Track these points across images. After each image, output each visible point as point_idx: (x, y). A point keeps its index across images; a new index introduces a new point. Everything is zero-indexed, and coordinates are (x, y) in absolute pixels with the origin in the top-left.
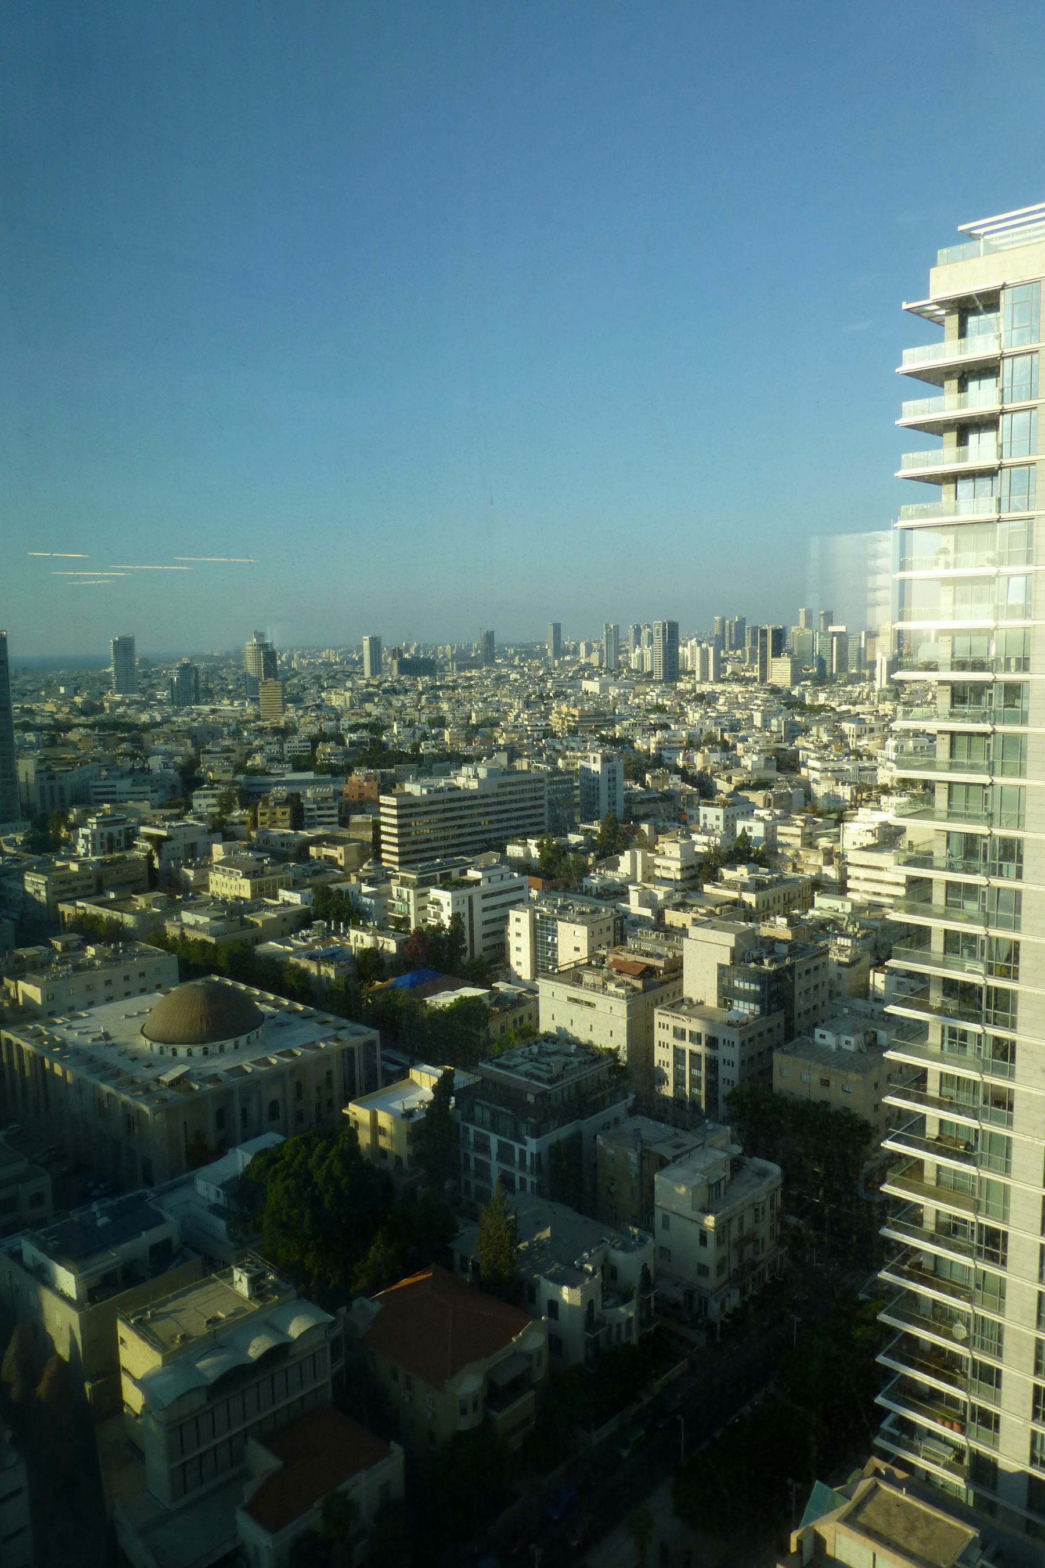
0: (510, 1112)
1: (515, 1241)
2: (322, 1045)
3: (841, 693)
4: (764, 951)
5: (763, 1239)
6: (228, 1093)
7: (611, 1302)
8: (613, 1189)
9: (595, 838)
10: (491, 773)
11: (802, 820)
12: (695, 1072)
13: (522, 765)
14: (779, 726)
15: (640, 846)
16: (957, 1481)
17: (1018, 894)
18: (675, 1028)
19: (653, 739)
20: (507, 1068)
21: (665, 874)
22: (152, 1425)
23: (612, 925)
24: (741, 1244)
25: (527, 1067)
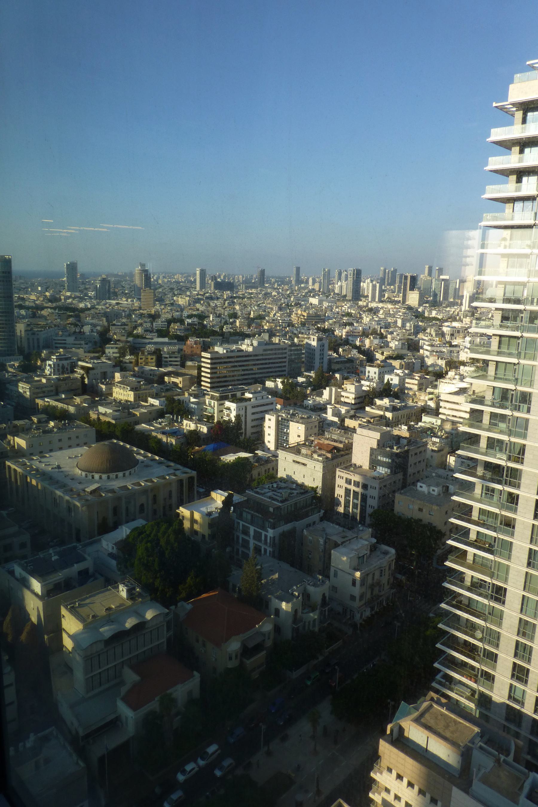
1: (260, 579)
2: (168, 477)
3: (444, 311)
4: (394, 442)
5: (384, 584)
6: (119, 499)
7: (305, 611)
8: (310, 556)
9: (311, 380)
10: (260, 344)
11: (419, 376)
12: (355, 501)
13: (276, 340)
14: (410, 327)
15: (335, 385)
16: (472, 705)
17: (527, 420)
18: (346, 479)
19: (344, 331)
20: (261, 494)
21: (347, 400)
22: (78, 658)
24: (372, 587)
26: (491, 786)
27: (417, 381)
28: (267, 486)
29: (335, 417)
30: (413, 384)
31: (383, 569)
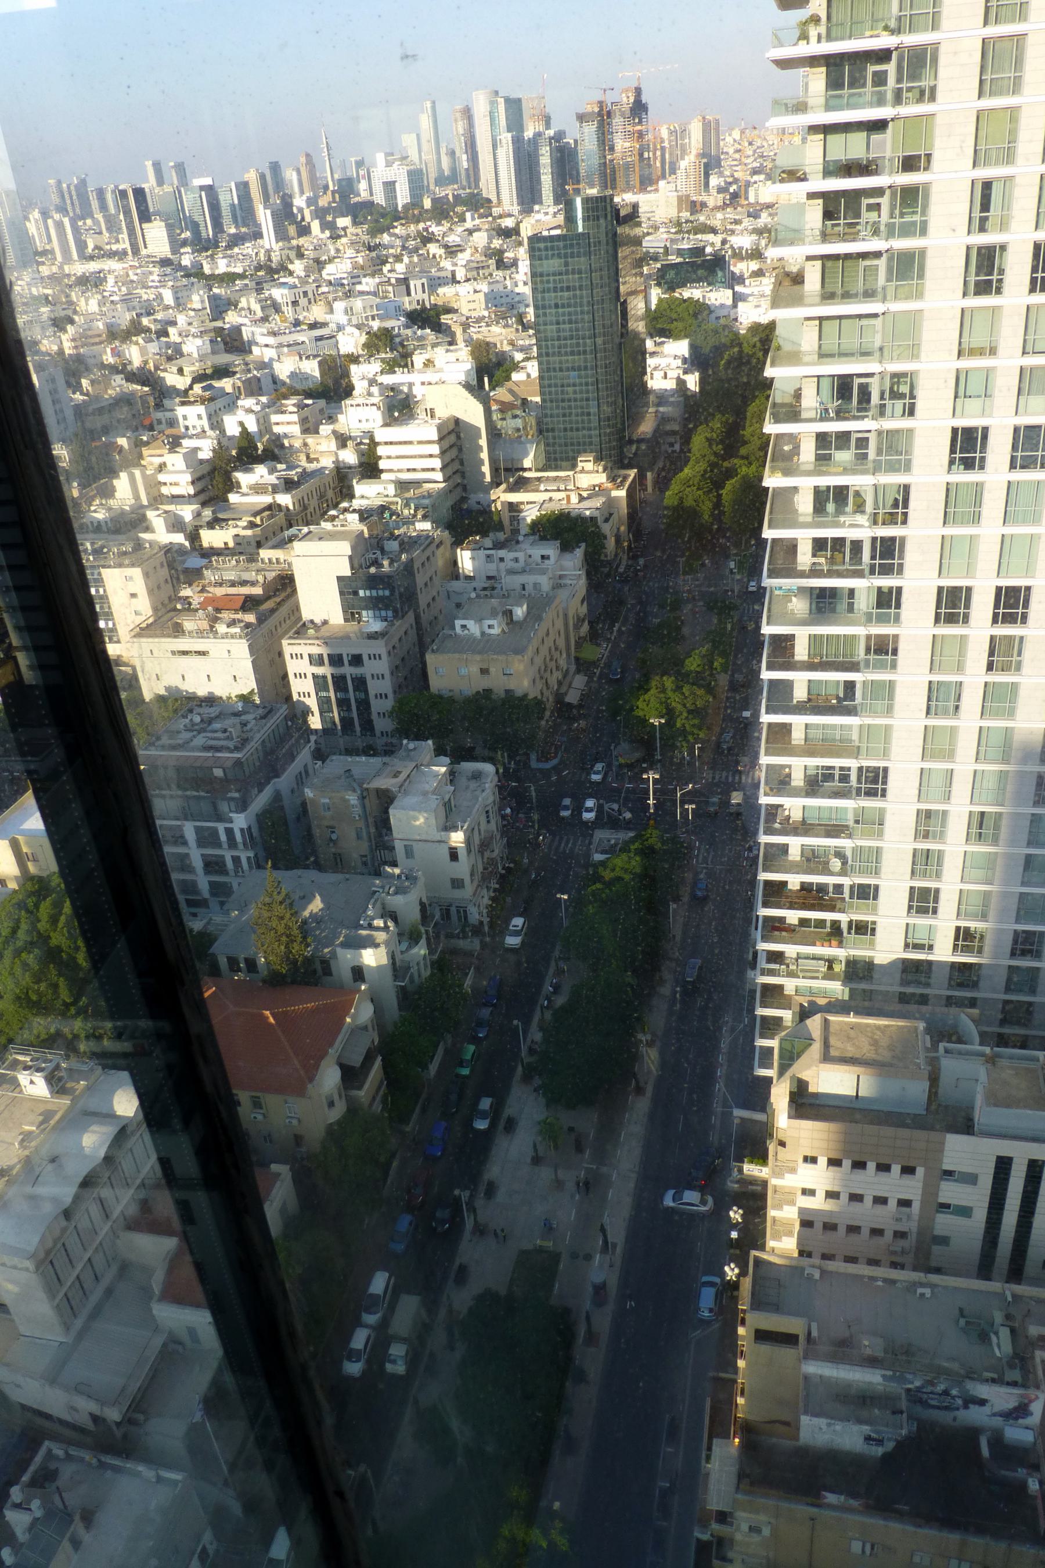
0: (202, 794)
3: (241, 257)
8: (334, 837)
11: (294, 405)
14: (202, 302)
19: (64, 337)
23: (163, 559)
25: (200, 740)
26: (1008, 1106)
27: (296, 416)
28: (182, 727)
29: (174, 532)
30: (288, 423)
31: (489, 808)
